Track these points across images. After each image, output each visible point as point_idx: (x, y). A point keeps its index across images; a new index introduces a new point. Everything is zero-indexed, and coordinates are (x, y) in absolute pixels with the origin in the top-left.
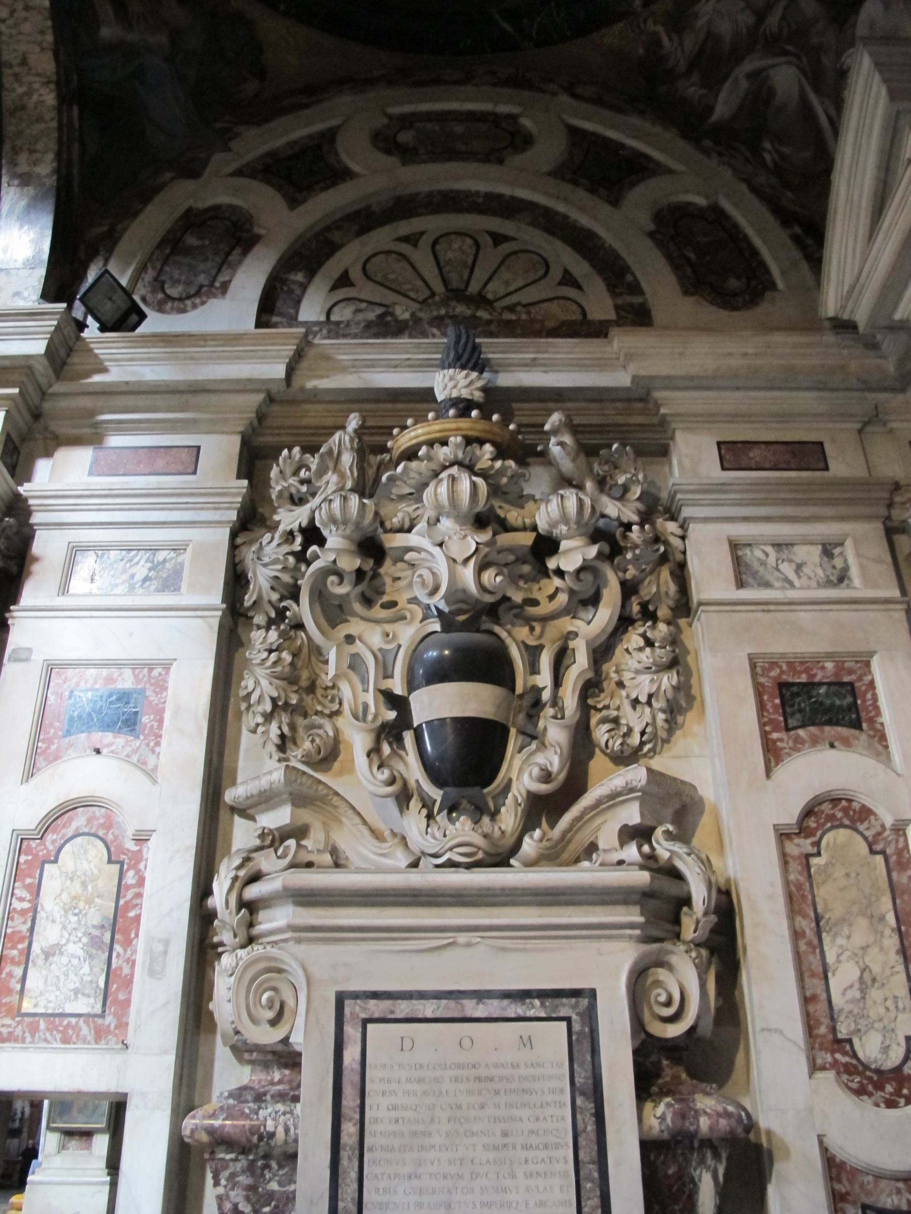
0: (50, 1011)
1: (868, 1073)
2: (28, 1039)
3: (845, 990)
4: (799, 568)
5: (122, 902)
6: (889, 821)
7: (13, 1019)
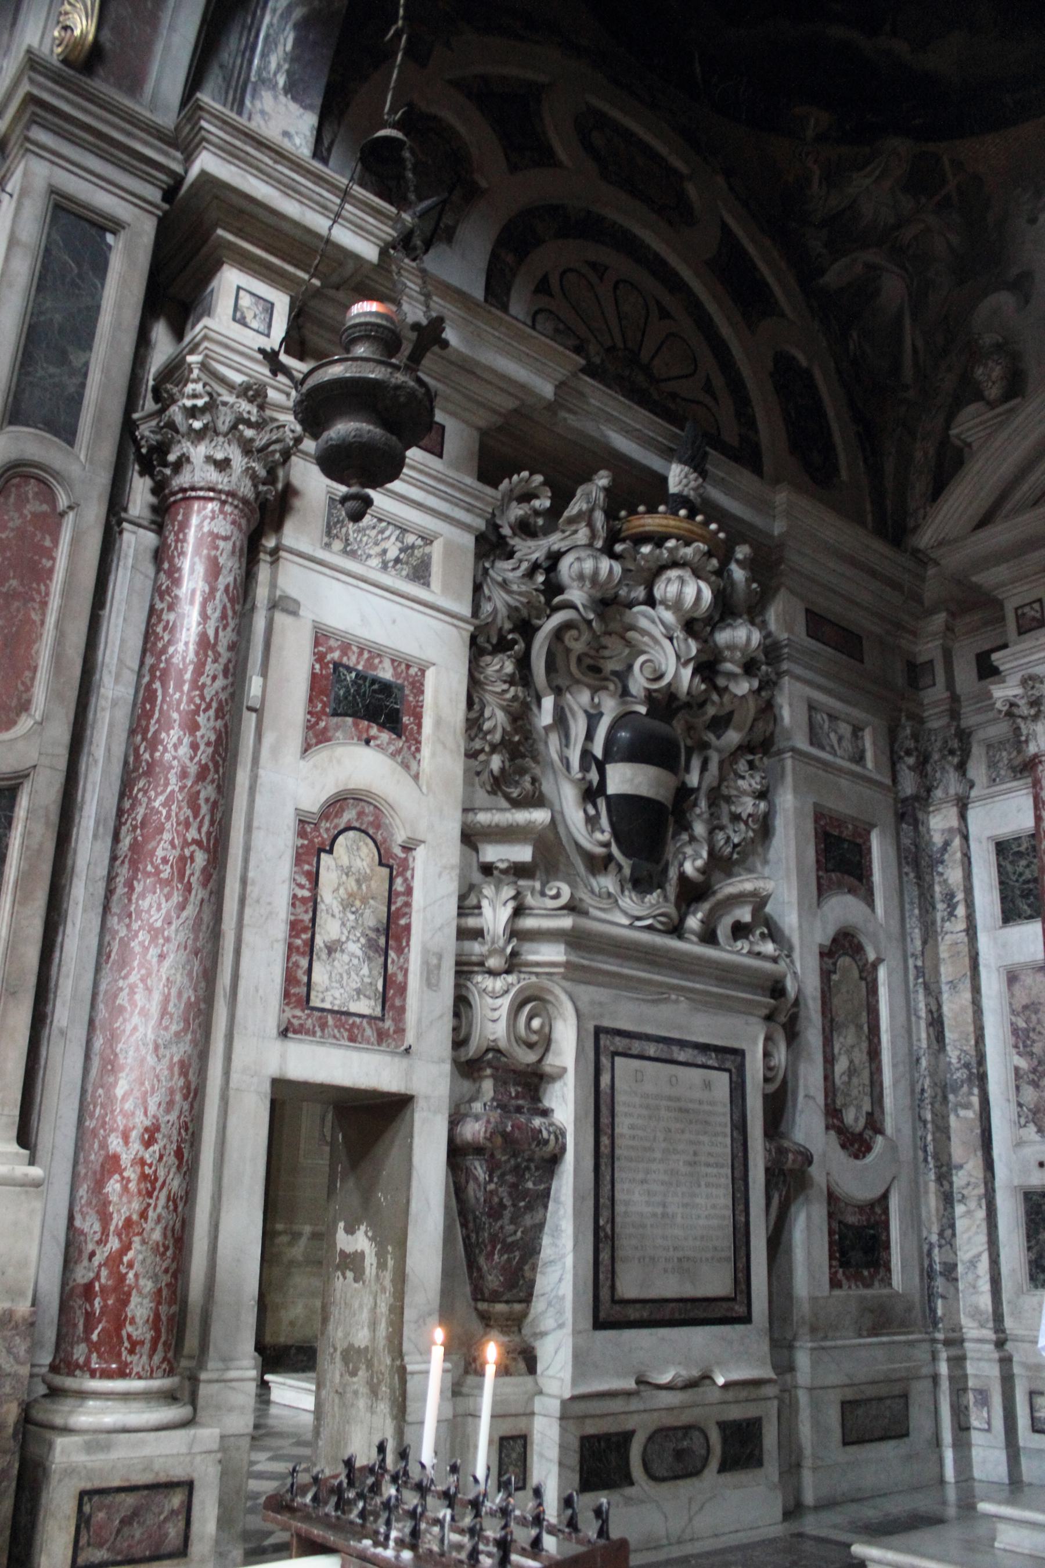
0: (336, 1008)
2: (319, 1034)
4: (840, 739)
5: (393, 908)
7: (303, 1010)
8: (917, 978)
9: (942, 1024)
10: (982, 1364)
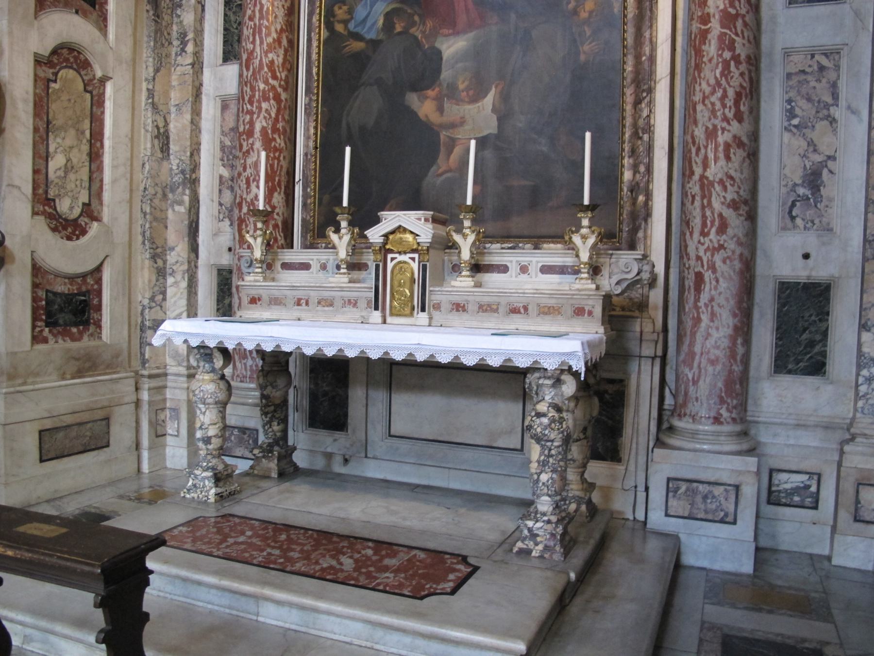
1: (60, 220)
3: (56, 170)
6: (99, 74)
8: (148, 98)
9: (168, 138)
10: (177, 391)
